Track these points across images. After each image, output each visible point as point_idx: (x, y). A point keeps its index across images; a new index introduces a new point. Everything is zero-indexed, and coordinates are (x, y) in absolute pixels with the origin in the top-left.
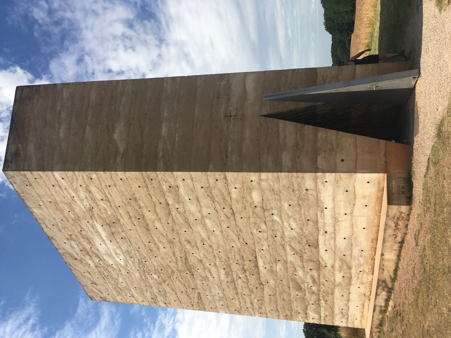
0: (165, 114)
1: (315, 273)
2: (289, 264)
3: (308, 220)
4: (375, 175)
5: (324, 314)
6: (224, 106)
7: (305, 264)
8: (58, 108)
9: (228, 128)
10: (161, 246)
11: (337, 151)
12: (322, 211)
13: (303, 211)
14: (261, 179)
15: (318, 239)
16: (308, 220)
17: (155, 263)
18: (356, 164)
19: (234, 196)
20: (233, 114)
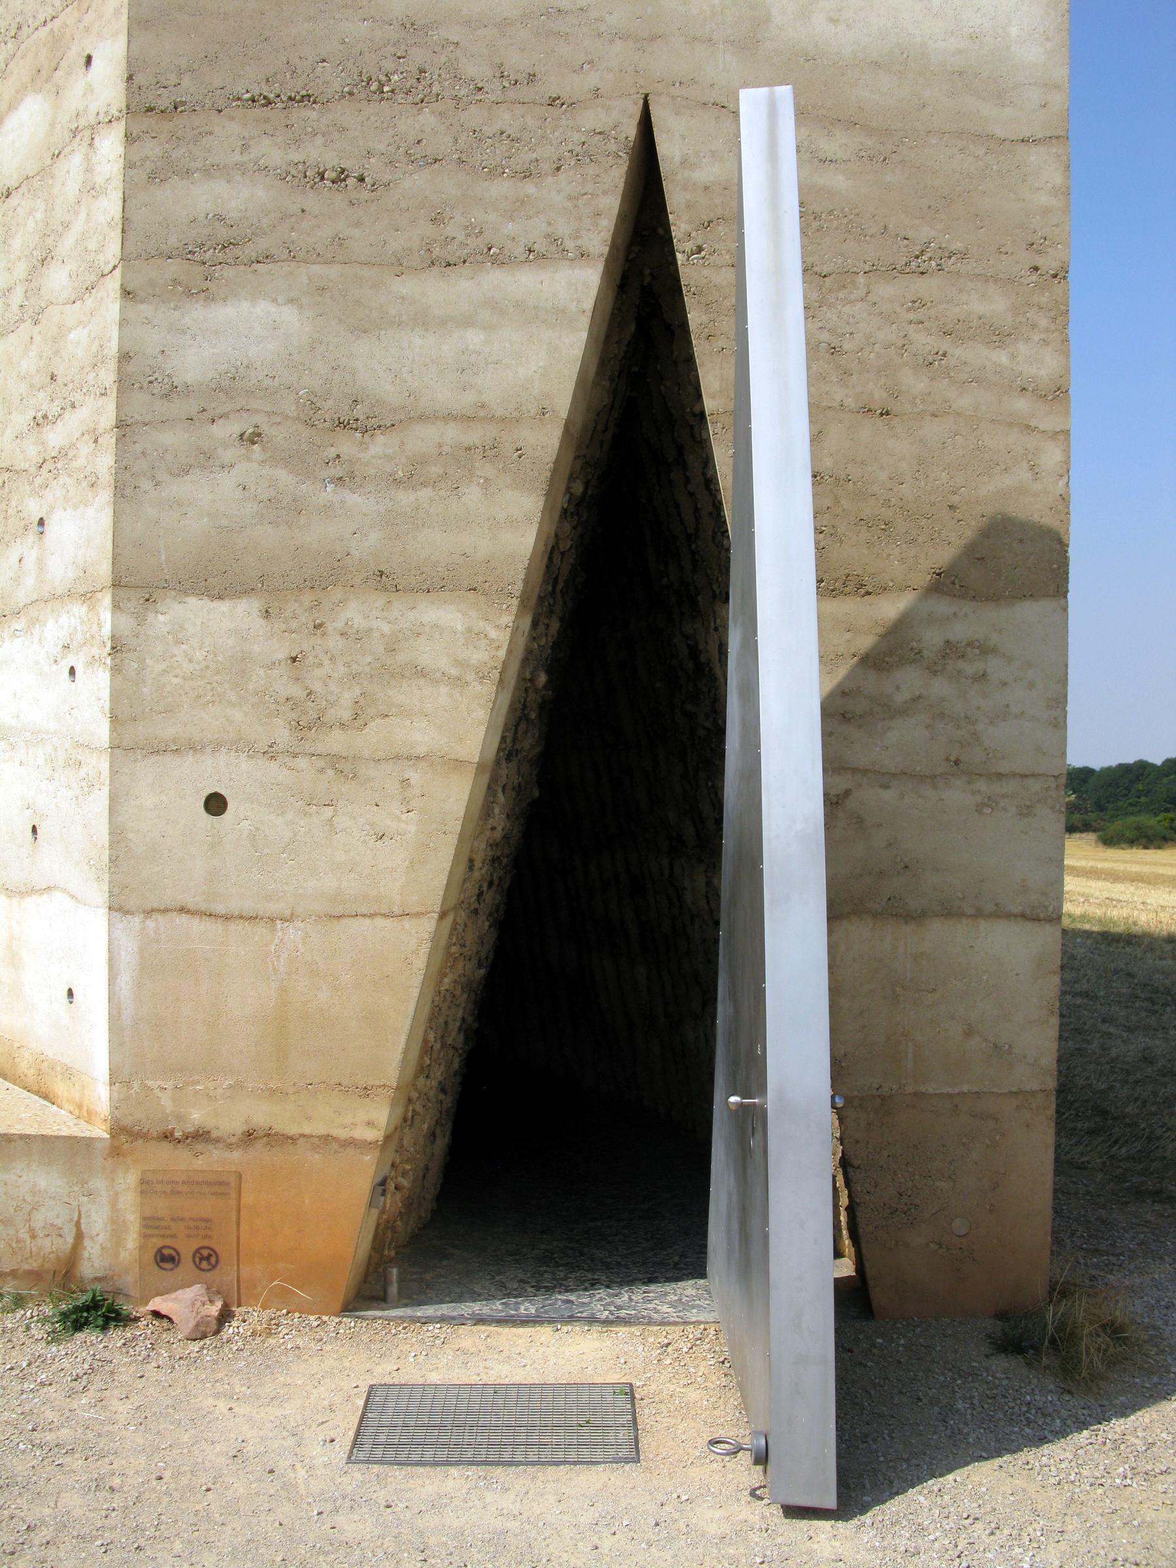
11: (302, 763)
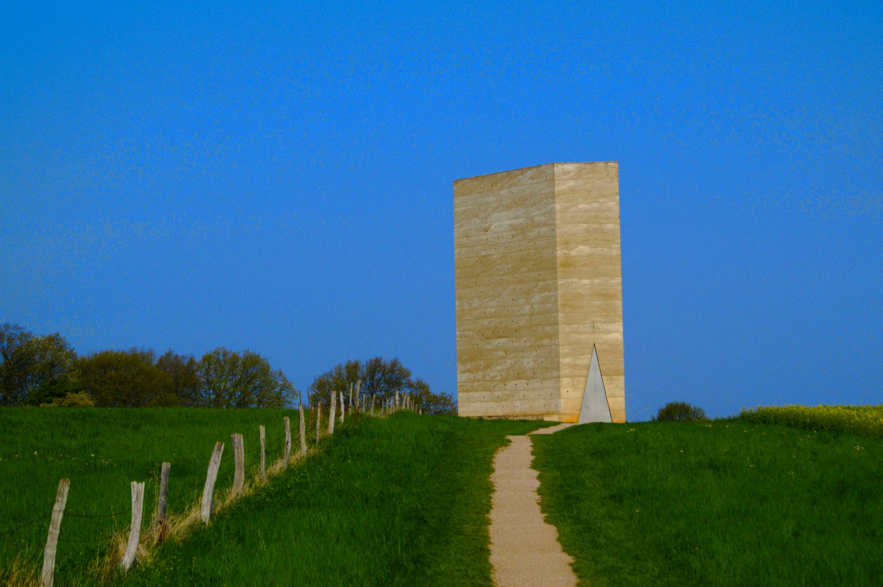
0: (595, 281)
1: (499, 378)
2: (504, 360)
5: (467, 385)
6: (600, 320)
7: (505, 371)
8: (600, 200)
10: (509, 266)
15: (523, 379)
17: (495, 257)
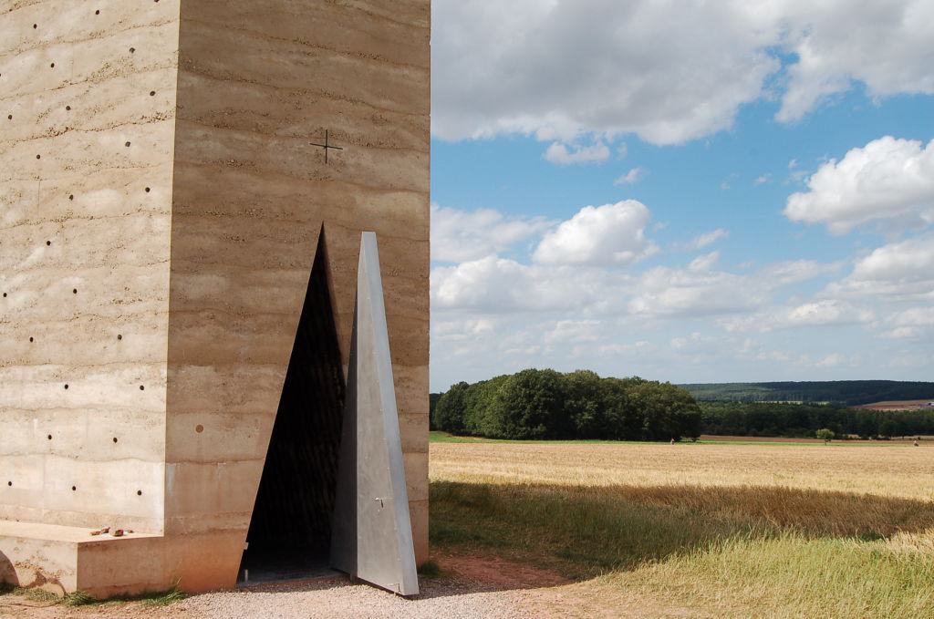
3: (32, 339)
4: (159, 509)
9: (295, 136)
12: (57, 377)
13: (60, 325)
14: (153, 217)
16: (32, 339)
18: (190, 461)
19: (105, 139)
20: (332, 153)
